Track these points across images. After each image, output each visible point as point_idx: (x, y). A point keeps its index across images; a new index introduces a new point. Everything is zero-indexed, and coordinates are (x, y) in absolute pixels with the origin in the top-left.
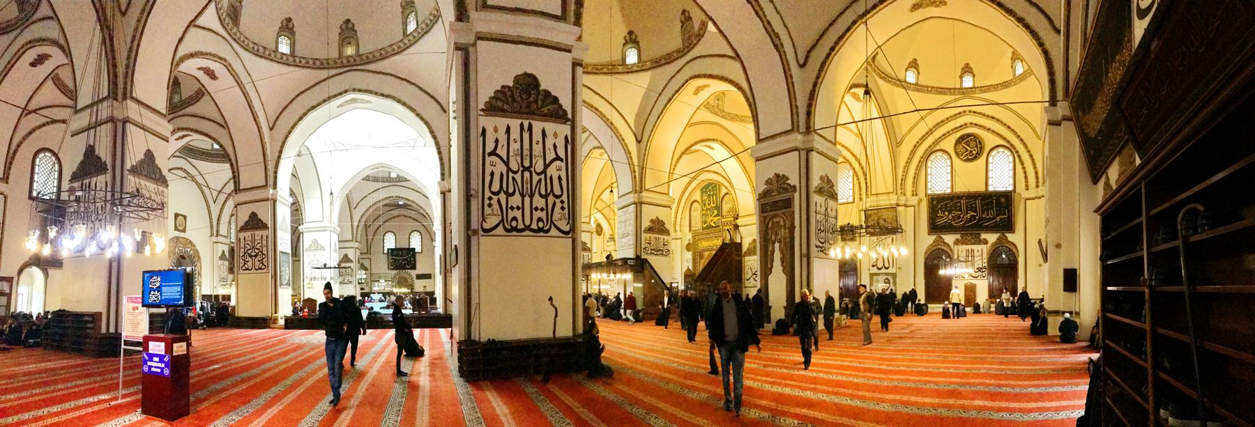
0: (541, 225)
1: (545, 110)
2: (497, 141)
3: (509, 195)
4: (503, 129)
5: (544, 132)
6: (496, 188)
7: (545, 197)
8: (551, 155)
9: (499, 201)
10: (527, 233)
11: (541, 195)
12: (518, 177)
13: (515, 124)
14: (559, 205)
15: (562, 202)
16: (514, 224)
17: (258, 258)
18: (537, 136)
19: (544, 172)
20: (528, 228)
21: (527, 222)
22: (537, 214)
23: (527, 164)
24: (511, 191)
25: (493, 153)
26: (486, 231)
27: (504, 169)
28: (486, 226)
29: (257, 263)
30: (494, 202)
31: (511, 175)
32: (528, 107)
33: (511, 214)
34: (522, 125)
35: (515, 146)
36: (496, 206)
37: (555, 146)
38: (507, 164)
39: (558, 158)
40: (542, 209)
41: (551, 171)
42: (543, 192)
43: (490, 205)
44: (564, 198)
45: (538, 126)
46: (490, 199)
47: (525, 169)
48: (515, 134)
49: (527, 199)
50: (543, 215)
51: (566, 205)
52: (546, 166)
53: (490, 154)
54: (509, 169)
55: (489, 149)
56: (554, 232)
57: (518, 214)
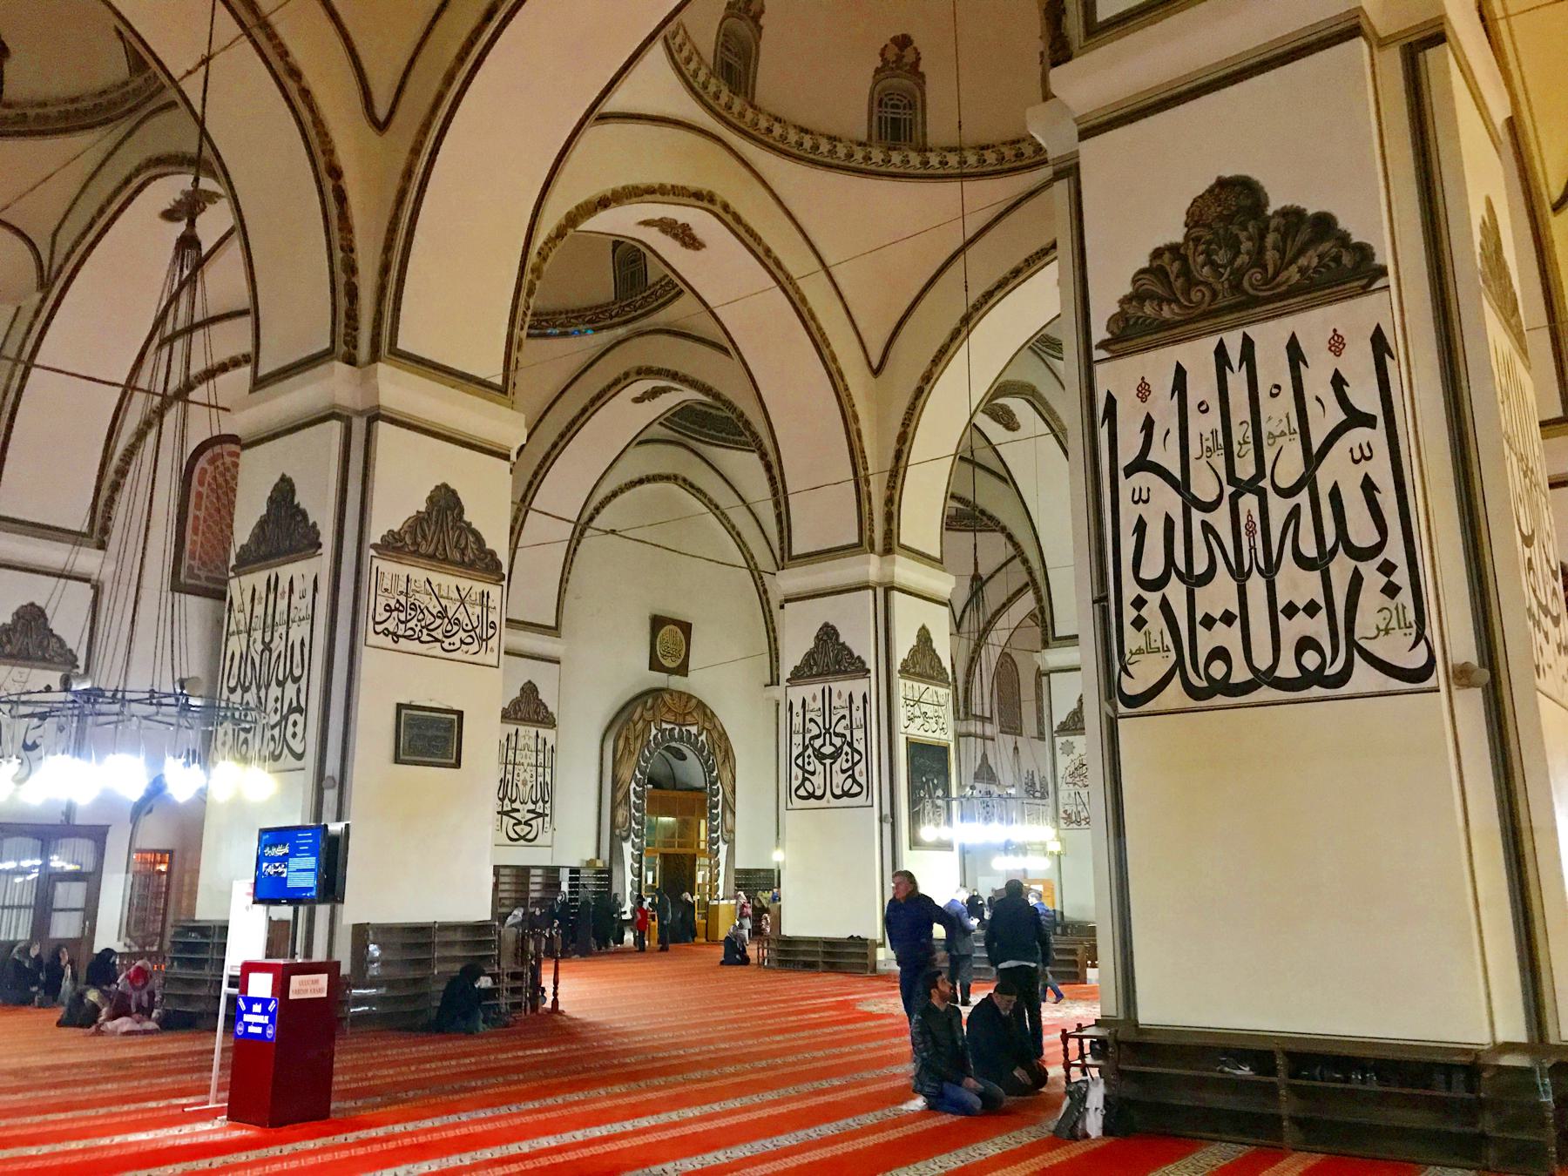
0: (1311, 660)
1: (1293, 274)
2: (1148, 425)
3: (1194, 582)
4: (1163, 383)
5: (1295, 354)
6: (1153, 568)
7: (1318, 564)
8: (1325, 419)
9: (1165, 605)
10: (1266, 693)
11: (1302, 561)
12: (1221, 520)
13: (1197, 355)
14: (1373, 579)
15: (1387, 568)
16: (1218, 669)
17: (841, 763)
18: (1273, 367)
19: (1307, 480)
20: (1268, 678)
21: (1263, 660)
22: (1291, 630)
23: (1245, 469)
24: (1200, 567)
25: (1142, 464)
26: (1133, 701)
27: (1171, 501)
28: (1131, 687)
29: (839, 778)
30: (1152, 611)
31: (1197, 516)
32: (1236, 287)
33: (1207, 641)
34: (1221, 352)
35: (1204, 425)
36: (1156, 622)
37: (1338, 382)
38: (1181, 486)
39: (1356, 419)
40: (1311, 609)
41: (1337, 470)
42: (1309, 549)
43: (1139, 623)
44: (1395, 551)
45: (1270, 337)
46: (1139, 603)
47: (1241, 487)
48: (1202, 387)
49: (1256, 585)
50: (1317, 627)
51: (1401, 577)
52: (1313, 460)
53: (1130, 471)
54: (1191, 502)
55: (1126, 457)
56: (1364, 677)
57: (1229, 637)
